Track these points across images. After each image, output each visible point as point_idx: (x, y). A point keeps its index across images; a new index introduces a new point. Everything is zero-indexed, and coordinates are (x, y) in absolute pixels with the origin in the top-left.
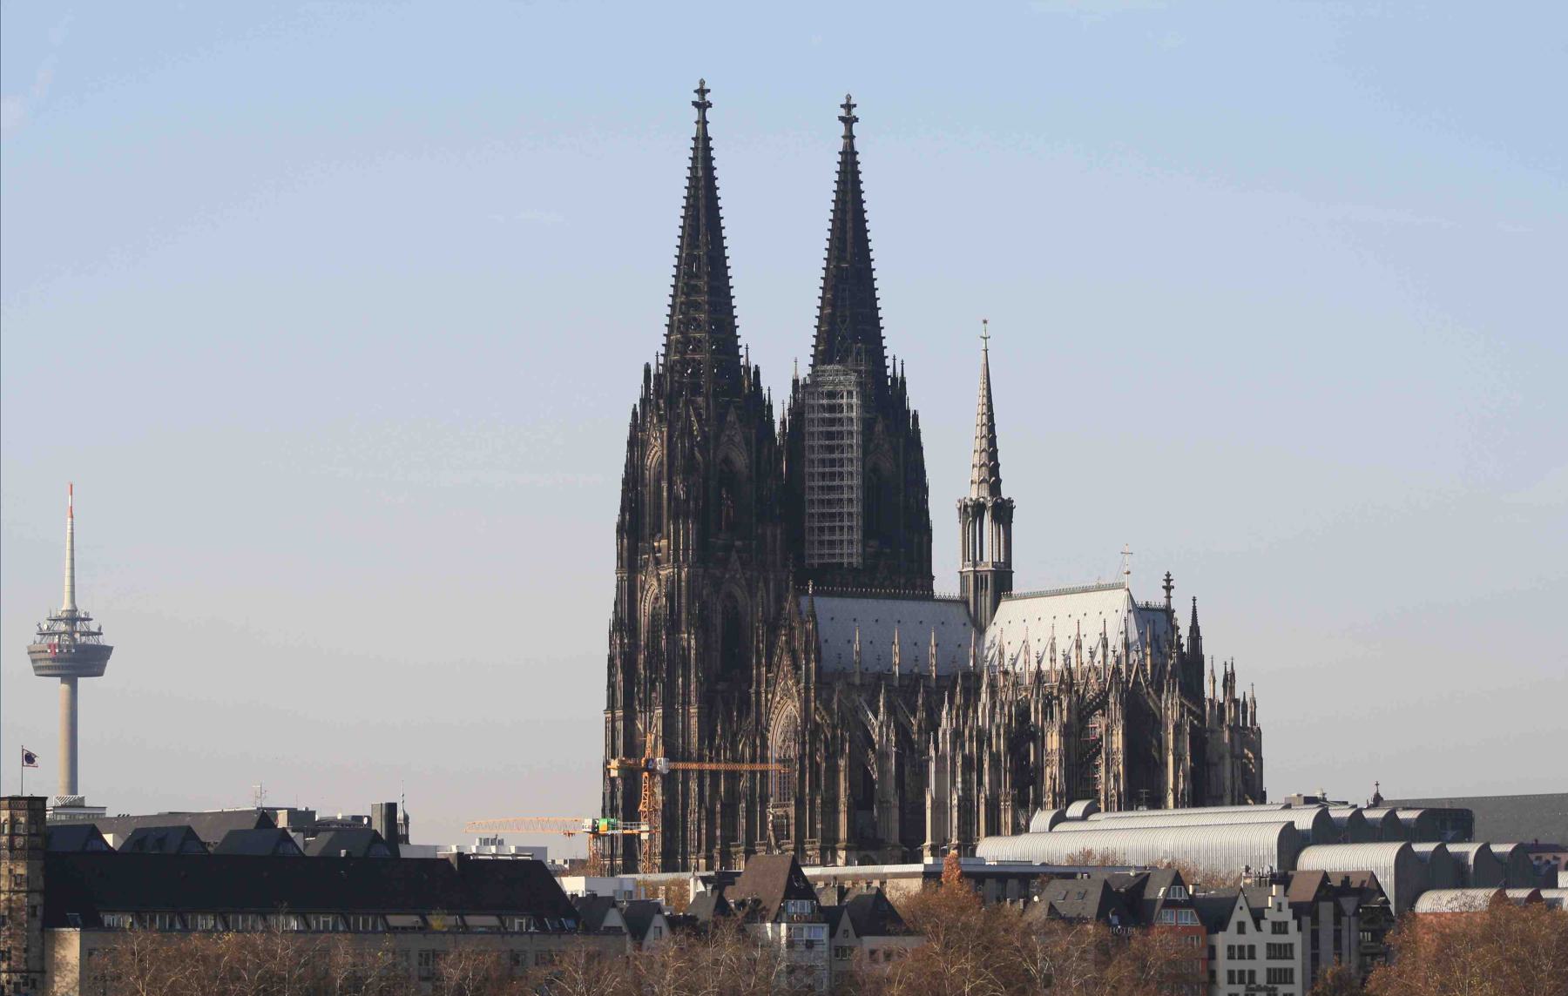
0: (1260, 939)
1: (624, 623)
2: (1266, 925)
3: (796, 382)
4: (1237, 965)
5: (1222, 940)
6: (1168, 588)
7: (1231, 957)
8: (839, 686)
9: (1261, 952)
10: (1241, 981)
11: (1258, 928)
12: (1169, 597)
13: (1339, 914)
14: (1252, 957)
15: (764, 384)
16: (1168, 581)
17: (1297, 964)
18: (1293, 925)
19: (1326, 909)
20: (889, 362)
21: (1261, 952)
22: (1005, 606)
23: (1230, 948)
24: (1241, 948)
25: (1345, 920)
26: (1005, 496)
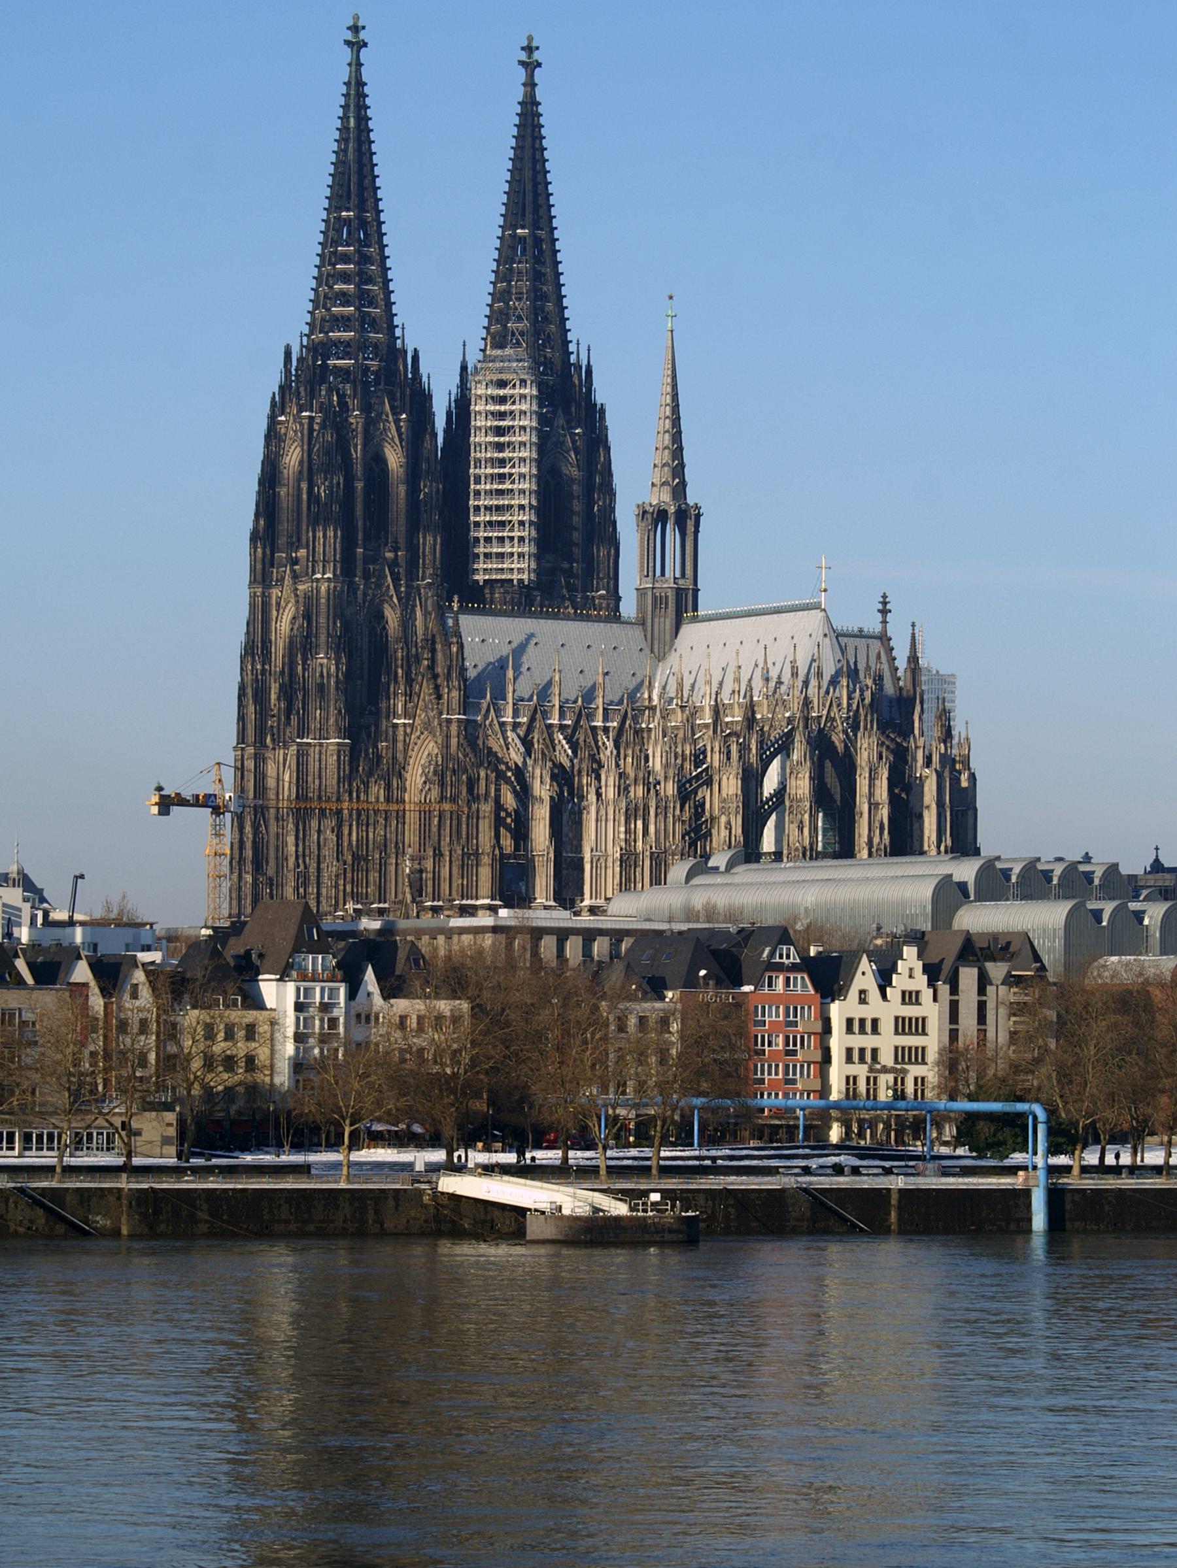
0: (887, 1010)
1: (256, 646)
2: (893, 993)
3: (464, 368)
4: (858, 1041)
5: (837, 1011)
6: (884, 612)
7: (849, 1029)
9: (887, 1026)
10: (862, 1060)
11: (884, 996)
12: (884, 622)
13: (983, 981)
14: (875, 1030)
15: (423, 370)
16: (885, 603)
17: (933, 1042)
18: (927, 994)
19: (968, 976)
20: (572, 347)
21: (887, 1026)
22: (689, 631)
23: (850, 1022)
24: (862, 1021)
25: (990, 990)
26: (691, 501)
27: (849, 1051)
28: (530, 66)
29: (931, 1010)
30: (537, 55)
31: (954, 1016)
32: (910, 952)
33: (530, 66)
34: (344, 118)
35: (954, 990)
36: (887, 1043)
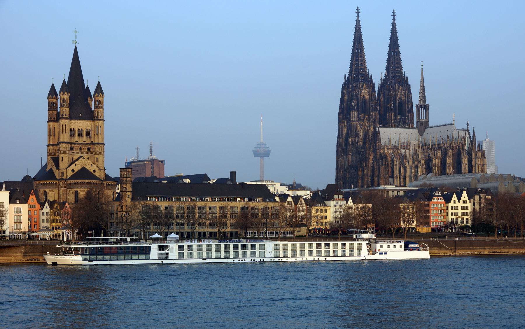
1: (339, 136)
2: (461, 201)
3: (381, 78)
4: (453, 211)
6: (468, 125)
7: (452, 209)
8: (386, 148)
9: (460, 208)
10: (455, 215)
11: (459, 202)
13: (480, 198)
14: (457, 209)
18: (468, 201)
22: (427, 130)
23: (452, 207)
24: (455, 207)
27: (452, 213)
29: (469, 204)
32: (465, 192)
34: (356, 28)
36: (460, 211)
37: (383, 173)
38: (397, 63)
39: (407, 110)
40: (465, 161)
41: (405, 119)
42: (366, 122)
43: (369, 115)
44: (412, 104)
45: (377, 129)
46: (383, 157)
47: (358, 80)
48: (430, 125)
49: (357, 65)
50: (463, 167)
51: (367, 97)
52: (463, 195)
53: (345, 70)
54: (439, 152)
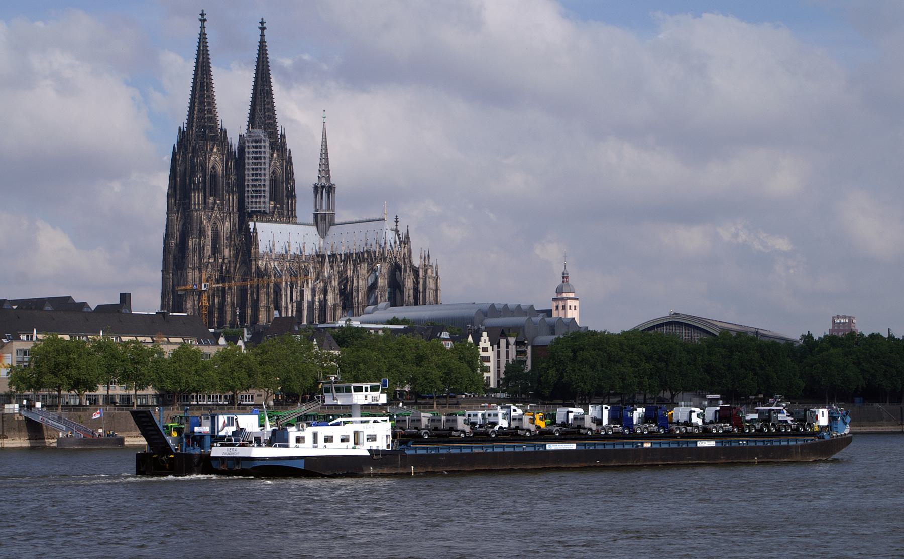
6: (397, 222)
18: (490, 348)
28: (263, 29)
30: (265, 25)
31: (499, 356)
32: (485, 334)
33: (263, 29)
34: (199, 47)
35: (499, 347)
37: (263, 302)
38: (269, 110)
39: (285, 192)
40: (409, 283)
41: (282, 208)
42: (216, 213)
43: (222, 200)
44: (294, 184)
45: (251, 225)
46: (261, 274)
47: (204, 137)
48: (337, 221)
49: (201, 111)
50: (406, 294)
51: (219, 168)
52: (482, 339)
53: (181, 119)
54: (365, 266)
